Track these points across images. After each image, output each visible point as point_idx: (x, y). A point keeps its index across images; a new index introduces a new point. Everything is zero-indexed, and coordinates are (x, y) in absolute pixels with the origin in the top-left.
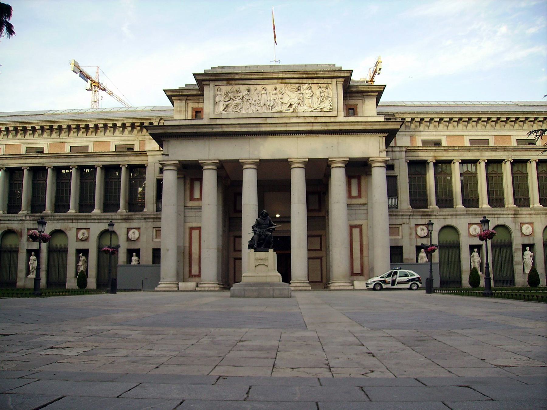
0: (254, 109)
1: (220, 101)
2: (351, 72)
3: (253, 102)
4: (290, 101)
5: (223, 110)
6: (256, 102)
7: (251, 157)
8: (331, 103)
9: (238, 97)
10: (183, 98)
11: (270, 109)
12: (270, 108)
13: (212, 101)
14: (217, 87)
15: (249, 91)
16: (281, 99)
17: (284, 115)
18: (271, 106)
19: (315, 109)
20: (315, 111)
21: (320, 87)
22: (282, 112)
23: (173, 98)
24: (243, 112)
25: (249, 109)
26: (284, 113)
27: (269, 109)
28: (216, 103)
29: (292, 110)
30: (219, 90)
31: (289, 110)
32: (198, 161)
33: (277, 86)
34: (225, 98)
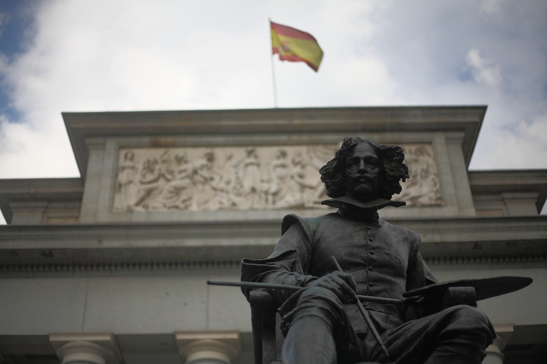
0: (225, 201)
1: (130, 182)
3: (222, 185)
5: (137, 204)
6: (233, 184)
7: (214, 325)
8: (438, 186)
9: (181, 172)
10: (39, 204)
12: (270, 198)
13: (107, 182)
14: (123, 153)
15: (211, 158)
18: (275, 194)
23: (12, 204)
24: (194, 208)
28: (117, 187)
30: (129, 156)
32: (47, 337)
34: (144, 176)
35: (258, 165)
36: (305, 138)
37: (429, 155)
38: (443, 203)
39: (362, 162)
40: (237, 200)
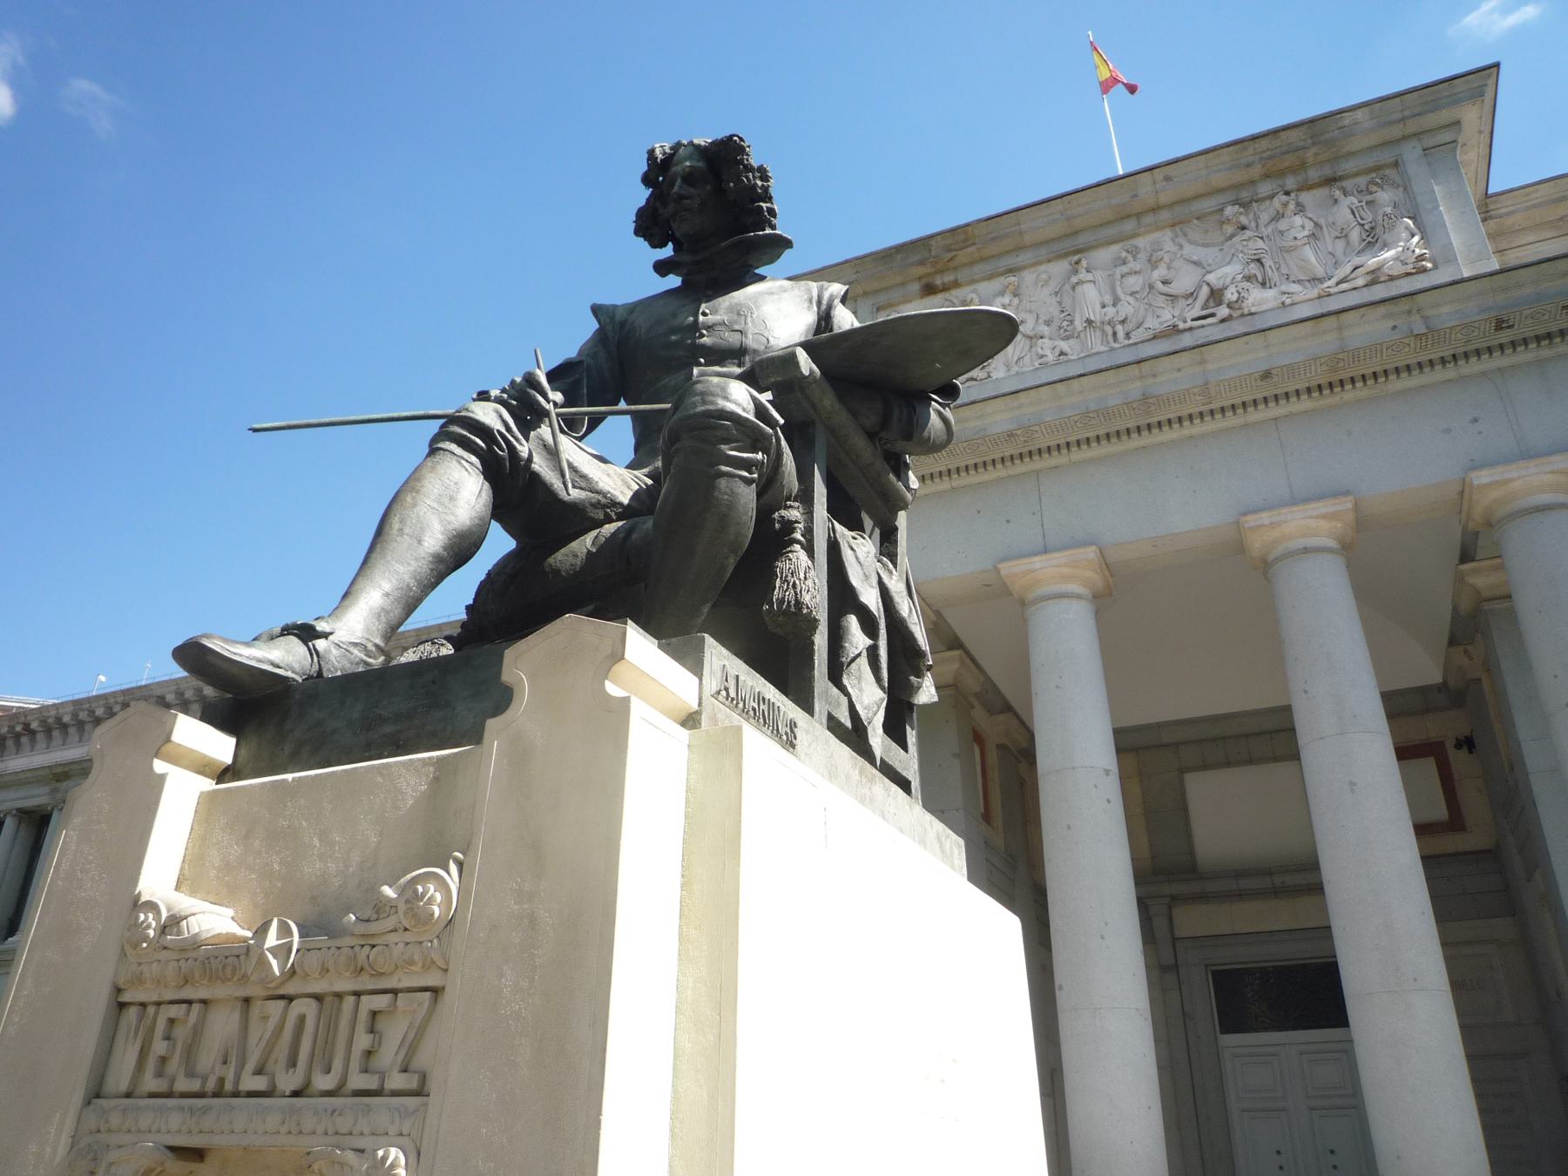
0: (1048, 352)
2: (1495, 69)
4: (1211, 278)
11: (1121, 335)
16: (1163, 283)
17: (1187, 340)
18: (1123, 322)
19: (1338, 284)
20: (1344, 286)
21: (1345, 194)
22: (1174, 330)
25: (1027, 360)
26: (1187, 334)
27: (1115, 334)
29: (1223, 311)
31: (1213, 315)
33: (1141, 242)
35: (1094, 282)
36: (1165, 215)
37: (1395, 185)
38: (1429, 265)
39: (679, 181)
40: (1064, 346)
